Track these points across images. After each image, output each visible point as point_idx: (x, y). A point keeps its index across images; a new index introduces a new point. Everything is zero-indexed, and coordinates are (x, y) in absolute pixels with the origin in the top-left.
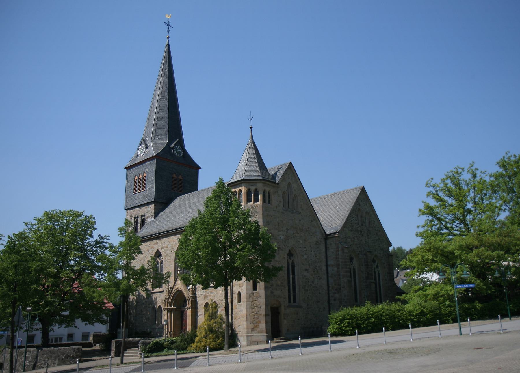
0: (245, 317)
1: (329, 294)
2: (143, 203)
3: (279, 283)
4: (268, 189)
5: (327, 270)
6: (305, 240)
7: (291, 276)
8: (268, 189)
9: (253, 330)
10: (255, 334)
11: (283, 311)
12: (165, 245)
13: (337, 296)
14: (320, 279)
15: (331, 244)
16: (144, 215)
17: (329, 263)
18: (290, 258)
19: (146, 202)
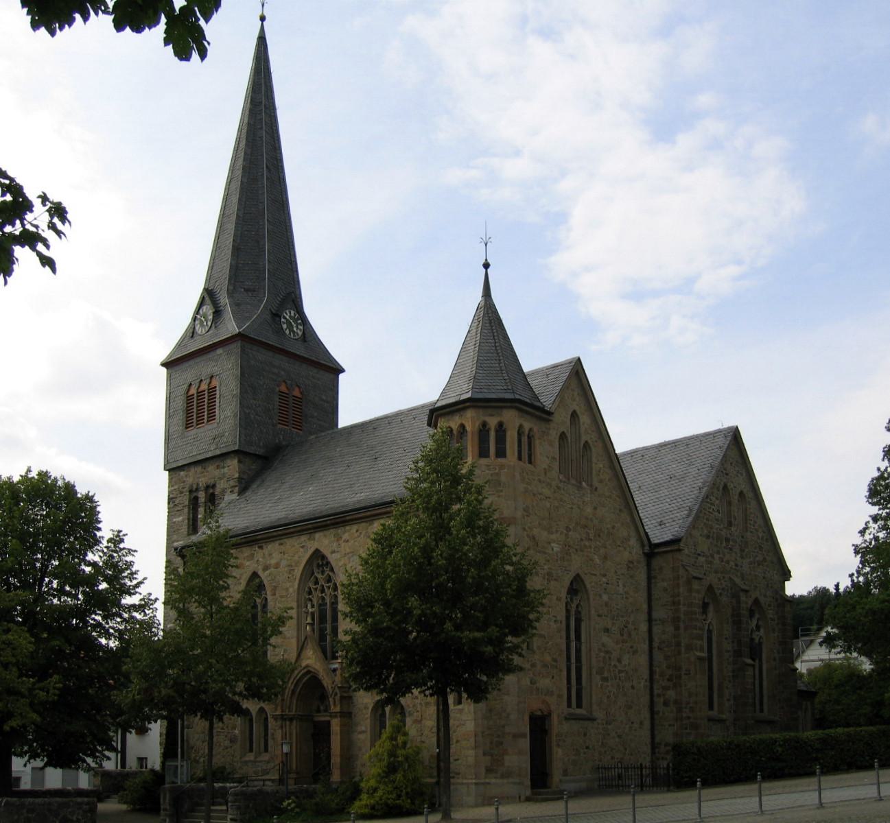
0: (472, 740)
1: (651, 689)
2: (210, 455)
3: (548, 658)
4: (527, 426)
5: (650, 631)
6: (605, 558)
7: (573, 644)
8: (527, 426)
9: (489, 770)
10: (493, 781)
11: (558, 727)
12: (273, 562)
13: (671, 694)
14: (635, 652)
15: (661, 569)
16: (214, 486)
17: (655, 615)
18: (571, 599)
19: (218, 452)
